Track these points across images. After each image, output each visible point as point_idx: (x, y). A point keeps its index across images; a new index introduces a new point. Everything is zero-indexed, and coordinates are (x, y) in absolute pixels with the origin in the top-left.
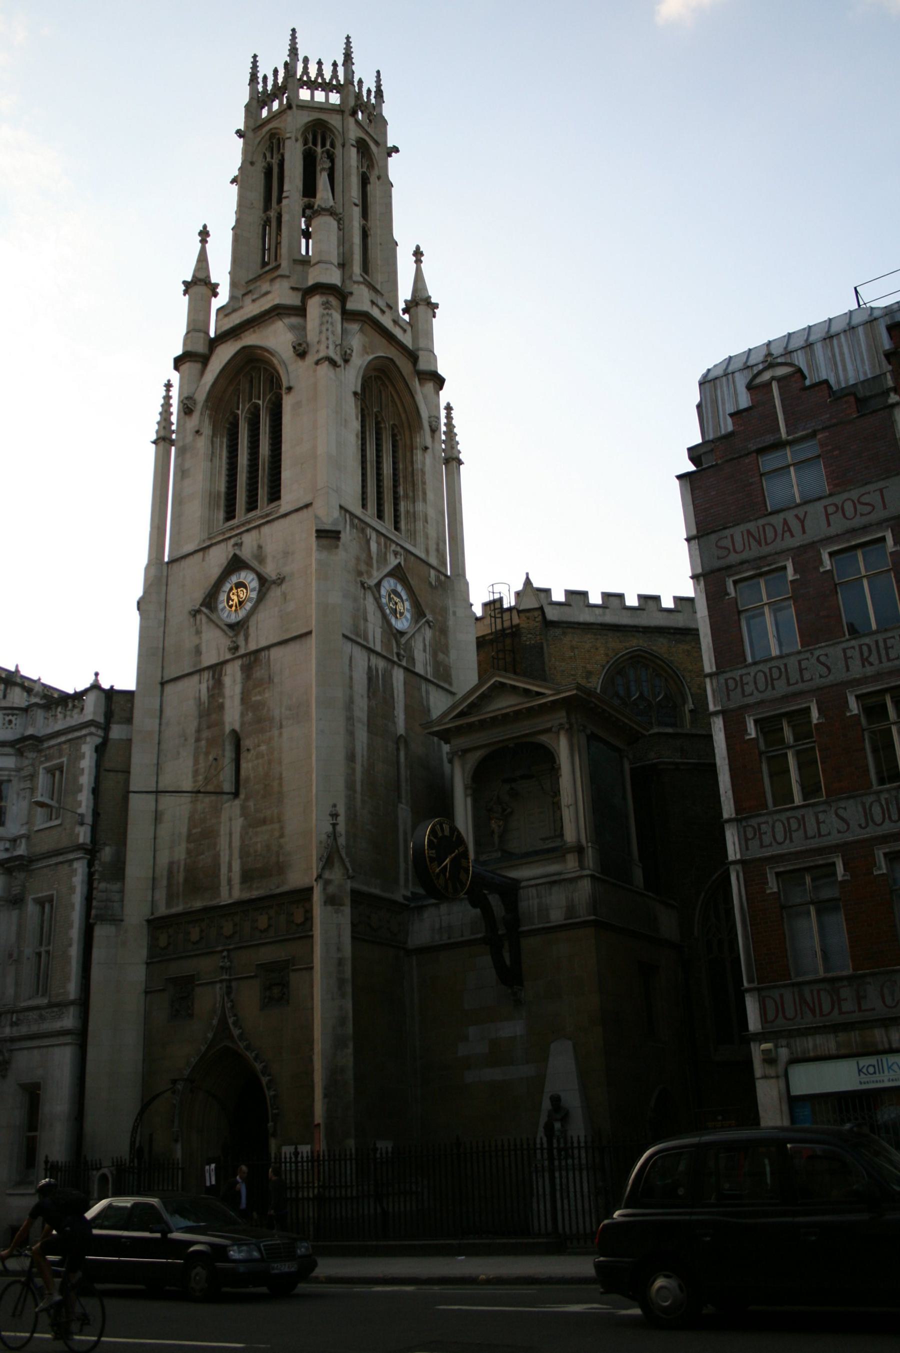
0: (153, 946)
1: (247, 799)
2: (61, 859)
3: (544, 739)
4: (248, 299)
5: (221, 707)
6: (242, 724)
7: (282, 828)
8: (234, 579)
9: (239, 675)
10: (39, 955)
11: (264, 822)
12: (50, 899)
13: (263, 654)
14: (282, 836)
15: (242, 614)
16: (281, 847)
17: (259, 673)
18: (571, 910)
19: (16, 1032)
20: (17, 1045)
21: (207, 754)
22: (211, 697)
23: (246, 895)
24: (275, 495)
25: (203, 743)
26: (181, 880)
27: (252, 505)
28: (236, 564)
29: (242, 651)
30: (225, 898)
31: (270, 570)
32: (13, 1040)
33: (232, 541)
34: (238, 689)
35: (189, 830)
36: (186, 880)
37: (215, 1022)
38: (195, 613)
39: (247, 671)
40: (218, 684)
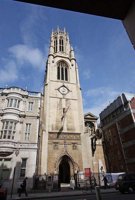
0: (49, 136)
1: (67, 118)
2: (33, 118)
3: (94, 123)
4: (63, 54)
5: (62, 104)
6: (66, 108)
8: (63, 88)
9: (65, 101)
12: (30, 124)
15: (64, 93)
17: (68, 102)
18: (99, 143)
19: (21, 147)
20: (20, 150)
21: (59, 110)
23: (68, 132)
24: (67, 79)
25: (59, 108)
26: (55, 127)
27: (63, 79)
30: (63, 131)
34: (65, 103)
35: (56, 120)
38: (56, 90)
39: (66, 101)
40: (61, 100)
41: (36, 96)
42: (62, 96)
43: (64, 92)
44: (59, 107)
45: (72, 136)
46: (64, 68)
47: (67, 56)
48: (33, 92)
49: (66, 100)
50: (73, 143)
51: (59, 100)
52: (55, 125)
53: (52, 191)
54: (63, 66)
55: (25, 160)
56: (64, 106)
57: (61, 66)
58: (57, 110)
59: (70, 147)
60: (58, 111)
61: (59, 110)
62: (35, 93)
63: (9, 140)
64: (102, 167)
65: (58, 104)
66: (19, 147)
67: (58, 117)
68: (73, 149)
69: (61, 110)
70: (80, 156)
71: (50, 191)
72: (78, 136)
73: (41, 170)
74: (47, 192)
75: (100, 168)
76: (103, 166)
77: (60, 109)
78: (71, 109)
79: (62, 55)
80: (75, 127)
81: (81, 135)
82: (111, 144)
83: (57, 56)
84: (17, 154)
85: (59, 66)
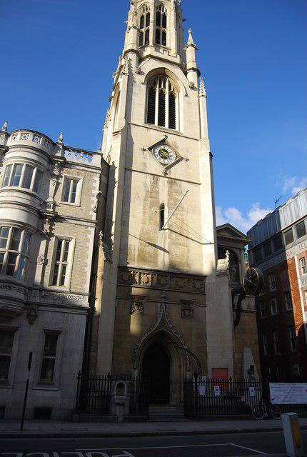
0: (119, 278)
2: (79, 222)
5: (158, 192)
7: (189, 250)
8: (162, 147)
9: (166, 184)
10: (57, 266)
11: (180, 244)
13: (178, 181)
14: (188, 253)
16: (188, 257)
17: (175, 187)
18: (249, 305)
19: (43, 301)
22: (152, 186)
24: (172, 125)
26: (136, 255)
27: (161, 123)
28: (163, 142)
29: (168, 176)
31: (182, 154)
32: (40, 305)
33: (162, 133)
34: (166, 189)
36: (139, 255)
37: (159, 319)
40: (156, 182)
41: (87, 163)
42: (160, 170)
43: (165, 158)
44: (150, 199)
45: (181, 282)
46: (167, 90)
47: (177, 60)
48: (79, 151)
49: (169, 182)
50: (184, 302)
51: (149, 180)
52: (137, 249)
53: (127, 420)
54: (164, 87)
55: (52, 338)
56: (163, 198)
57: (160, 86)
58: (144, 208)
59: (175, 311)
60: (147, 208)
61: (150, 207)
62: (85, 153)
63: (9, 278)
64: (252, 367)
65: (147, 191)
66: (38, 300)
67: (146, 227)
68: (184, 316)
69: (153, 209)
70: (202, 337)
71: (120, 419)
72: (198, 284)
73: (96, 364)
74: (114, 421)
75: (246, 367)
76: (253, 364)
77: (152, 205)
78: (183, 208)
79: (165, 56)
80: (191, 258)
81: (207, 281)
82: (275, 312)
83: (151, 56)
84: (32, 318)
85: (155, 84)
